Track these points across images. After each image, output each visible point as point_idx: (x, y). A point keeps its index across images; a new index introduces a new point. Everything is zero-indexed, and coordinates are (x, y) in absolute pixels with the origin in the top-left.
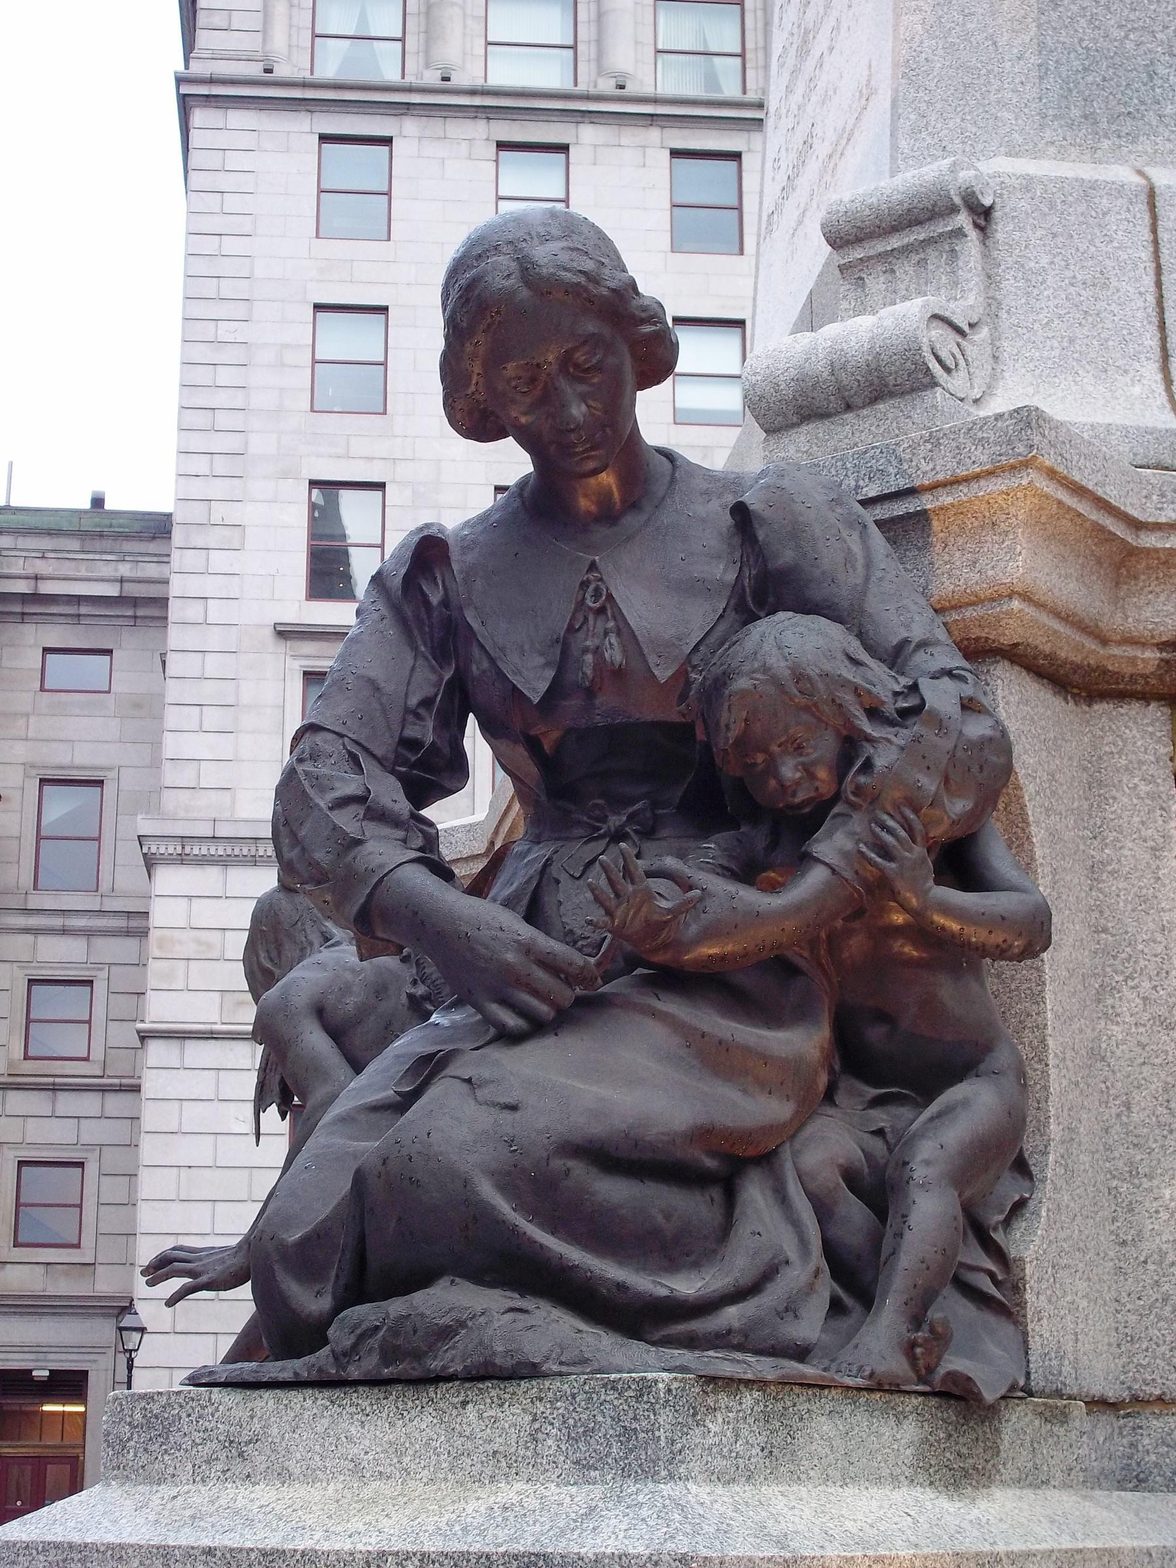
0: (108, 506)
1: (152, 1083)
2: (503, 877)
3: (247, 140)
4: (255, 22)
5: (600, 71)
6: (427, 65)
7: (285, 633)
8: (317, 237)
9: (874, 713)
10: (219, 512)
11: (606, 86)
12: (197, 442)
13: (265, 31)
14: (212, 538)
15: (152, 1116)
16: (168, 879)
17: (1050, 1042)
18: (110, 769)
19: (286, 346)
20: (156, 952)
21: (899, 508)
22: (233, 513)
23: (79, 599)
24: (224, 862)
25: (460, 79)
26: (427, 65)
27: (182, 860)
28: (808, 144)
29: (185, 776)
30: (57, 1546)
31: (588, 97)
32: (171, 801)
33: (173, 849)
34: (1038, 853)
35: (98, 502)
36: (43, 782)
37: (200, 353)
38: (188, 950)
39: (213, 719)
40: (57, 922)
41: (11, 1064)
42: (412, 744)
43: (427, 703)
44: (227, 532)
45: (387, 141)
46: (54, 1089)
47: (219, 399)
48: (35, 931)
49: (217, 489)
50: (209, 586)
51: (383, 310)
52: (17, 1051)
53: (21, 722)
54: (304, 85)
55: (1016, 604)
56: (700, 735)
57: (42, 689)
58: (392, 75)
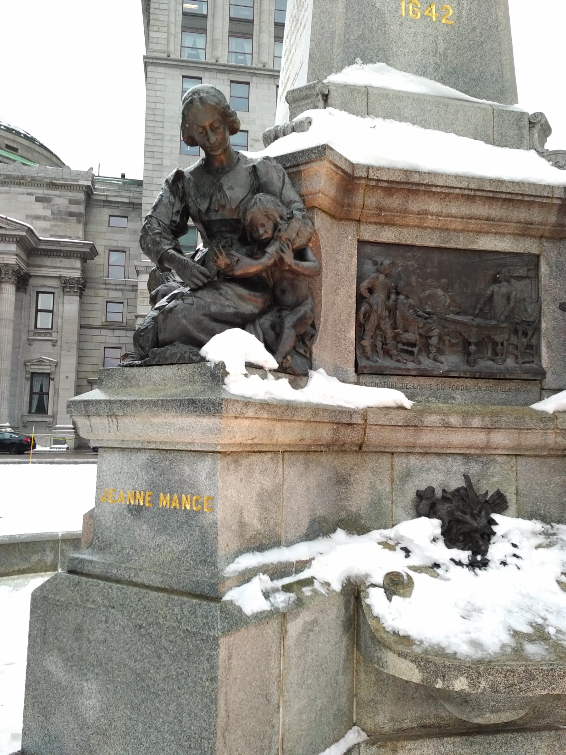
0: (126, 177)
2: (198, 255)
3: (162, 76)
5: (259, 62)
6: (212, 57)
9: (281, 218)
11: (260, 66)
12: (149, 161)
17: (323, 300)
18: (128, 248)
19: (173, 136)
20: (140, 296)
21: (294, 170)
23: (118, 202)
26: (212, 57)
28: (289, 77)
30: (86, 401)
31: (255, 69)
34: (323, 256)
35: (123, 176)
36: (110, 251)
37: (150, 136)
40: (114, 287)
41: (102, 322)
42: (175, 222)
43: (178, 212)
46: (114, 329)
47: (155, 149)
48: (109, 289)
49: (156, 174)
52: (104, 320)
53: (103, 235)
54: (178, 61)
55: (320, 195)
56: (242, 221)
57: (109, 226)
58: (203, 60)
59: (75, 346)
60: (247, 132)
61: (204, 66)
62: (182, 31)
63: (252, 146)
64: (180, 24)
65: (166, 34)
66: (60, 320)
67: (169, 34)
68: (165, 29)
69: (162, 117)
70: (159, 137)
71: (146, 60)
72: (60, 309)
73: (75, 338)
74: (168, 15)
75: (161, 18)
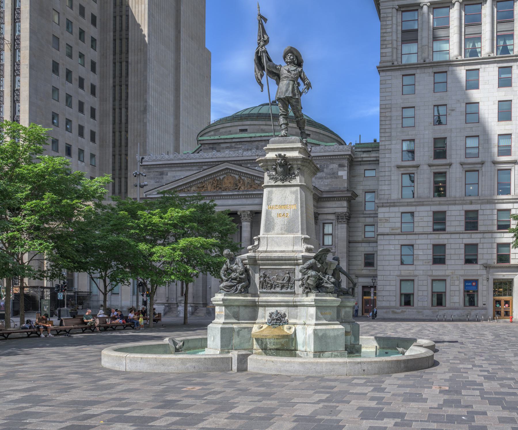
1: (379, 242)
3: (390, 78)
4: (390, 54)
7: (399, 167)
8: (402, 94)
10: (387, 147)
12: (383, 135)
13: (392, 56)
14: (386, 151)
15: (380, 248)
16: (381, 210)
22: (390, 147)
24: (390, 206)
25: (427, 61)
27: (383, 206)
29: (383, 193)
32: (380, 196)
33: (381, 205)
38: (384, 221)
39: (387, 183)
44: (388, 151)
45: (414, 75)
47: (387, 127)
49: (387, 143)
50: (386, 160)
51: (414, 107)
59: (346, 255)
60: (446, 105)
61: (416, 66)
62: (402, 44)
63: (449, 114)
64: (400, 40)
65: (391, 49)
66: (336, 240)
67: (392, 48)
68: (390, 46)
69: (390, 105)
70: (388, 118)
71: (379, 69)
72: (336, 233)
73: (345, 250)
74: (392, 36)
75: (388, 38)
